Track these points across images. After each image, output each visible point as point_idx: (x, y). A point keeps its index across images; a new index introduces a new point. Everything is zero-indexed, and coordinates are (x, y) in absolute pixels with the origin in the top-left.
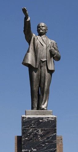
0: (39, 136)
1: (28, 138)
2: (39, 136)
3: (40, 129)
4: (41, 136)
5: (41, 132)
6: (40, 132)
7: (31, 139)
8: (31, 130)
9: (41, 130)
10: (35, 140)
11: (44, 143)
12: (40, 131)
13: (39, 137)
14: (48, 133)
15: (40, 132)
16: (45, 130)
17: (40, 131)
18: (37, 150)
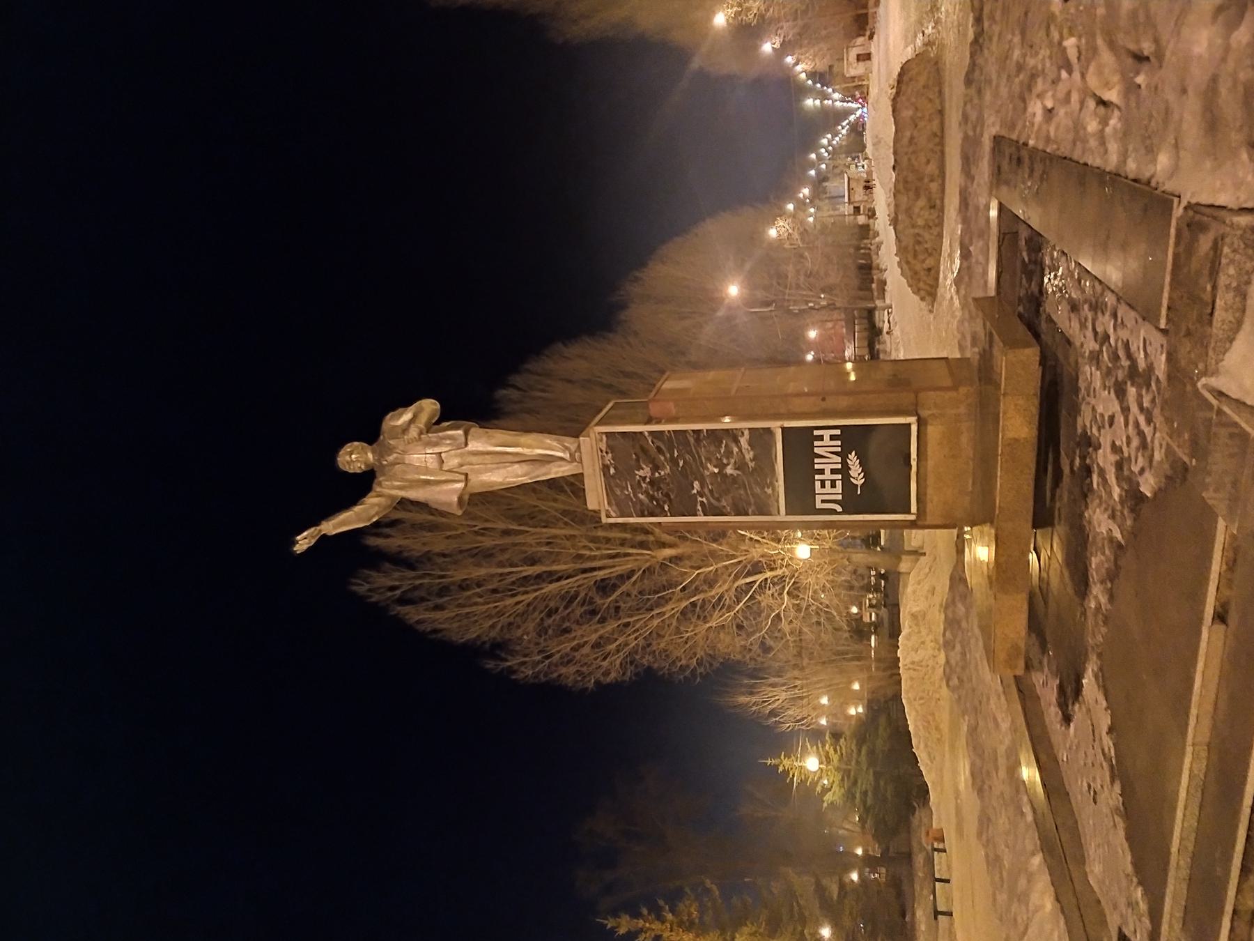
0: (657, 475)
1: (665, 502)
2: (657, 475)
3: (637, 472)
4: (656, 468)
5: (643, 469)
6: (645, 471)
7: (667, 495)
8: (641, 496)
9: (639, 471)
10: (668, 485)
11: (674, 462)
12: (641, 473)
13: (660, 474)
14: (644, 450)
15: (645, 471)
16: (638, 460)
17: (641, 473)
18: (696, 479)
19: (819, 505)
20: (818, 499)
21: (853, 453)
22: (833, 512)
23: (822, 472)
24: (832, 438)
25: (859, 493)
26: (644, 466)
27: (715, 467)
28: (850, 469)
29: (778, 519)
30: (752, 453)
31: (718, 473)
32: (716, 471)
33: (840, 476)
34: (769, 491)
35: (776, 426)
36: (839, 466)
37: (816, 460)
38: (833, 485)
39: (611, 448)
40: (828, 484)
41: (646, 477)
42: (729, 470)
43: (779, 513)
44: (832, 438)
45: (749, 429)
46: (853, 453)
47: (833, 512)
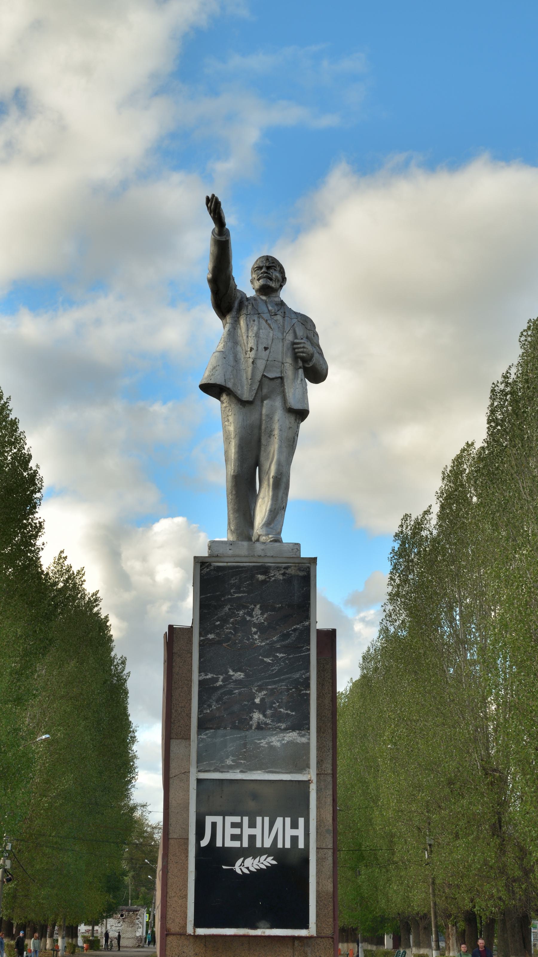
0: (254, 630)
1: (218, 634)
3: (258, 606)
7: (228, 639)
8: (227, 609)
13: (255, 633)
18: (247, 675)
19: (209, 820)
20: (218, 819)
21: (274, 862)
22: (200, 835)
23: (252, 825)
24: (294, 839)
25: (224, 867)
26: (265, 616)
27: (262, 700)
28: (254, 858)
29: (193, 770)
30: (278, 744)
31: (254, 703)
32: (257, 701)
33: (245, 844)
34: (229, 762)
35: (311, 775)
36: (259, 845)
37: (267, 819)
38: (234, 837)
39: (289, 580)
40: (237, 831)
41: (252, 617)
42: (257, 716)
43: (199, 771)
44: (294, 839)
45: (308, 744)
46: (274, 862)
47: (200, 835)
